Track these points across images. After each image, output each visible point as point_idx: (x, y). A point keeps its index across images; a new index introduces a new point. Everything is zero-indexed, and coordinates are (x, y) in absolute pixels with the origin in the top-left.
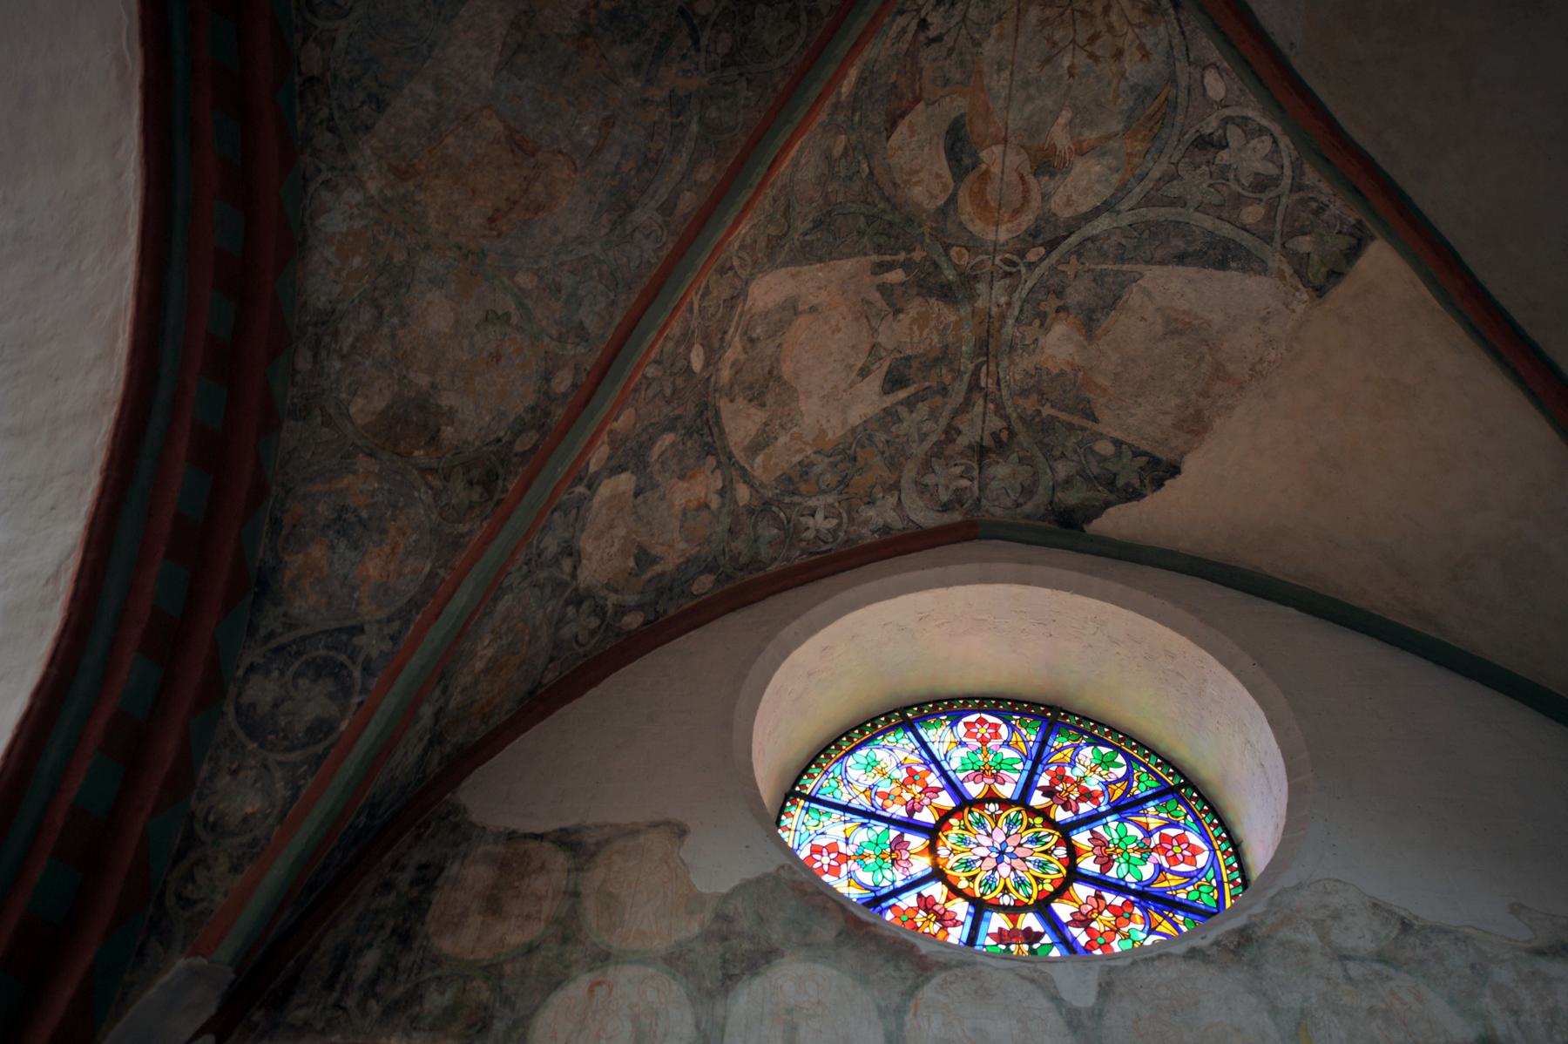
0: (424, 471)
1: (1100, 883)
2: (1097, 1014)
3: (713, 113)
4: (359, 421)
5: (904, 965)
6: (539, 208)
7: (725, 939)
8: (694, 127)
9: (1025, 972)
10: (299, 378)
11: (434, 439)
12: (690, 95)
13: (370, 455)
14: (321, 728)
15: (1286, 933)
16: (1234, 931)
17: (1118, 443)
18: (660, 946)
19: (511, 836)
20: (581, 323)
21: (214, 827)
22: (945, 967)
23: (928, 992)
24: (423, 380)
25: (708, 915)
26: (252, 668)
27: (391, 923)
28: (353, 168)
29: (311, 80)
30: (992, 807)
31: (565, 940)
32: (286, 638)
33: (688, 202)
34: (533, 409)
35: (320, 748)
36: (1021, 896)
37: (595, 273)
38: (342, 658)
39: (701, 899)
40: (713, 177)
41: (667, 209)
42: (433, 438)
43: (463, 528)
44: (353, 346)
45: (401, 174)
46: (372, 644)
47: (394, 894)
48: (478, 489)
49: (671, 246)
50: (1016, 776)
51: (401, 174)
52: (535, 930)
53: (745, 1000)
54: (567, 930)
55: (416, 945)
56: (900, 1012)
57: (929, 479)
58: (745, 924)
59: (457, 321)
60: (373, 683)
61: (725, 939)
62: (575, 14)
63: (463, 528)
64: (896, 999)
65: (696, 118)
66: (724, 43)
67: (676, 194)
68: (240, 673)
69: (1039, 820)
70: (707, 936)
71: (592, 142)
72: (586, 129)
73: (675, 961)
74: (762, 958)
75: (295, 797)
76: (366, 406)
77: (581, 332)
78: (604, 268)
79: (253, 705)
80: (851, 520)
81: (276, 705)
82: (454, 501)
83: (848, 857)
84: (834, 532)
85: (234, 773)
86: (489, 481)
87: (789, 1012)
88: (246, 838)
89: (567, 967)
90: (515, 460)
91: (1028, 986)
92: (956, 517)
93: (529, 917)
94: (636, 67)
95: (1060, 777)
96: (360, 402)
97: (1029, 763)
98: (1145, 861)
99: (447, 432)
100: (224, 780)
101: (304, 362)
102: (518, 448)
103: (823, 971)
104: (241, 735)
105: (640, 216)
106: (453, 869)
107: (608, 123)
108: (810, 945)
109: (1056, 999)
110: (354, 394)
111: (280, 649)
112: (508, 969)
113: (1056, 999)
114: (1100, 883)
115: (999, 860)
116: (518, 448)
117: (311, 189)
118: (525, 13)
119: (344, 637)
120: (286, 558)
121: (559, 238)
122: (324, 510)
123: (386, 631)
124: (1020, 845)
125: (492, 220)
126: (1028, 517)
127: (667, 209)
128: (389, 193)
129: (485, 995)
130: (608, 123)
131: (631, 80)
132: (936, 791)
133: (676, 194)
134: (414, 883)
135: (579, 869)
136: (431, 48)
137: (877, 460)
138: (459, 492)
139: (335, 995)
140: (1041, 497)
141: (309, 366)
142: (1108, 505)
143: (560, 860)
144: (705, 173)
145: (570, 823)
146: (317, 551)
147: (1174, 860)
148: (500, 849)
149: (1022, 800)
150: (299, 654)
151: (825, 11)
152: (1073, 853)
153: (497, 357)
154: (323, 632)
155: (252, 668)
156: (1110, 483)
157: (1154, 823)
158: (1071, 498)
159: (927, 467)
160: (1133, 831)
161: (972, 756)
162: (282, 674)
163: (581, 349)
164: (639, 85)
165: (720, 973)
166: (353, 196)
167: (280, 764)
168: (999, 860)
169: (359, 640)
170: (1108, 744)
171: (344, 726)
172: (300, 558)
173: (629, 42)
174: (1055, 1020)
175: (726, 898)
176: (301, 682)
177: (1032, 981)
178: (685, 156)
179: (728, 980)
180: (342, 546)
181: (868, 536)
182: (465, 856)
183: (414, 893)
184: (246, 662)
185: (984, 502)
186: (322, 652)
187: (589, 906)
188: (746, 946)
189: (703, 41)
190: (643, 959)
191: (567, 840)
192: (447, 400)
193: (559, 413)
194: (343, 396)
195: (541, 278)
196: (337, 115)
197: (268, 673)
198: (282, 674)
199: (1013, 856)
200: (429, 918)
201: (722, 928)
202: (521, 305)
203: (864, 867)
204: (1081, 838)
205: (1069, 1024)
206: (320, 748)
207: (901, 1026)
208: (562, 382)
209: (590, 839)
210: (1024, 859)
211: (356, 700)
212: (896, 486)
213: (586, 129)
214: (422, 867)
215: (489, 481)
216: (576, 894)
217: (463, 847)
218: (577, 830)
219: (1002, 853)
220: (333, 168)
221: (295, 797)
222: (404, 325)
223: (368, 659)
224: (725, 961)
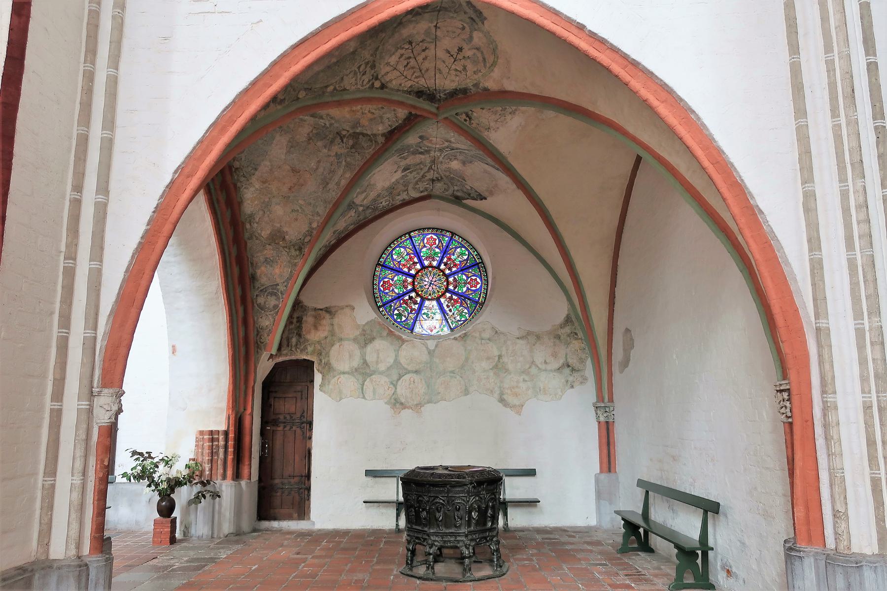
0: (283, 247)
1: (453, 293)
2: (434, 351)
3: (348, 159)
4: (264, 237)
5: (400, 341)
6: (302, 185)
7: (364, 335)
8: (344, 163)
9: (423, 342)
10: (248, 231)
11: (284, 239)
12: (341, 154)
13: (269, 245)
14: (275, 307)
15: (474, 334)
16: (463, 334)
17: (472, 188)
18: (352, 337)
19: (315, 309)
20: (318, 212)
21: (262, 329)
22: (407, 341)
23: (404, 346)
24: (278, 225)
25: (361, 330)
26: (257, 296)
27: (295, 332)
28: (251, 183)
29: (237, 169)
30: (430, 269)
31: (332, 336)
32: (262, 288)
33: (344, 183)
34: (308, 231)
35: (277, 310)
36: (433, 296)
37: (320, 200)
38: (275, 291)
39: (359, 325)
40: (350, 176)
41: (338, 184)
42: (284, 239)
43: (296, 261)
44: (259, 220)
45: (264, 182)
46: (281, 288)
47: (294, 325)
48: (298, 251)
49: (340, 194)
50: (438, 259)
51: (264, 182)
52: (326, 334)
53: (369, 348)
54: (332, 333)
55: (302, 337)
56: (398, 350)
57: (417, 186)
58: (368, 332)
59: (284, 212)
60: (284, 296)
61: (364, 335)
62: (306, 135)
63: (296, 261)
64: (398, 348)
65: (344, 160)
66: (351, 142)
67: (340, 181)
68: (255, 297)
69: (441, 273)
70: (361, 335)
71: (315, 167)
72: (313, 164)
73: (355, 340)
74: (372, 339)
75: (275, 321)
76: (265, 233)
77: (318, 214)
78: (322, 199)
79: (260, 304)
80: (393, 200)
81: (265, 303)
82: (293, 254)
83: (392, 285)
84: (388, 205)
85: (261, 318)
86: (300, 249)
87: (378, 350)
88: (268, 330)
89: (334, 341)
90: (306, 244)
91: (422, 345)
92: (426, 193)
93: (324, 330)
94: (325, 147)
95: (449, 259)
96: (263, 232)
97: (442, 254)
98: (465, 286)
99: (287, 237)
100: (260, 320)
101: (248, 226)
102: (306, 241)
103: (384, 342)
104: (260, 310)
105: (330, 186)
106: (305, 318)
107: (319, 162)
108: (381, 337)
109: (427, 348)
110: (262, 231)
111: (261, 291)
112: (322, 342)
113: (427, 348)
114: (453, 293)
115: (430, 286)
116: (306, 241)
117: (241, 190)
118: (292, 138)
119: (275, 287)
120: (256, 271)
121: (309, 192)
122: (262, 259)
123: (284, 285)
124: (435, 281)
125: (290, 189)
126: (446, 195)
127: (338, 184)
128: (261, 187)
129: (319, 348)
130: (319, 162)
131: (324, 150)
132: (417, 263)
133: (340, 181)
134: (297, 322)
135: (332, 318)
136: (267, 153)
137: (401, 186)
138: (294, 253)
139: (290, 348)
140: (450, 192)
141: (249, 227)
142: (468, 199)
143: (327, 316)
144: (348, 175)
145: (327, 306)
146: (263, 268)
147: (472, 287)
148: (313, 313)
149: (438, 267)
150: (266, 291)
151: (380, 143)
152: (448, 283)
153: (296, 219)
154: (270, 286)
155: (257, 296)
156: (469, 195)
157: (470, 275)
158: (459, 194)
159: (417, 183)
160: (464, 277)
161: (427, 251)
162: (264, 296)
163: (319, 218)
164: (326, 151)
165: (364, 343)
166: (252, 189)
167: (270, 314)
168: (430, 286)
169: (278, 287)
170: (465, 247)
171: (280, 306)
172: (259, 270)
173: (322, 140)
174: (426, 352)
175: (364, 325)
176: (268, 297)
177: (423, 344)
178: (342, 171)
179: (366, 344)
180: (268, 266)
181: (398, 203)
182: (306, 315)
183: (298, 325)
184: (255, 295)
185: (434, 190)
186: (271, 290)
187: (336, 327)
188: (369, 337)
189: (344, 141)
190: (348, 339)
191: (328, 310)
192: (285, 229)
193: (315, 232)
194: (259, 232)
195: (305, 201)
196: (245, 173)
197: (261, 296)
198: (264, 296)
199: (433, 284)
200: (303, 330)
201: (364, 332)
202: (301, 208)
203: (396, 288)
204: (451, 279)
205: (429, 353)
206: (277, 310)
207: (398, 353)
208: (315, 225)
209: (333, 310)
210: (436, 286)
211: (281, 300)
212: (407, 190)
213: (313, 164)
214: (298, 318)
215: (300, 249)
216: (333, 325)
217: (305, 312)
218: (330, 307)
219: (431, 283)
220: (246, 184)
221: (275, 321)
222: (271, 213)
223: (281, 291)
224: (365, 340)
